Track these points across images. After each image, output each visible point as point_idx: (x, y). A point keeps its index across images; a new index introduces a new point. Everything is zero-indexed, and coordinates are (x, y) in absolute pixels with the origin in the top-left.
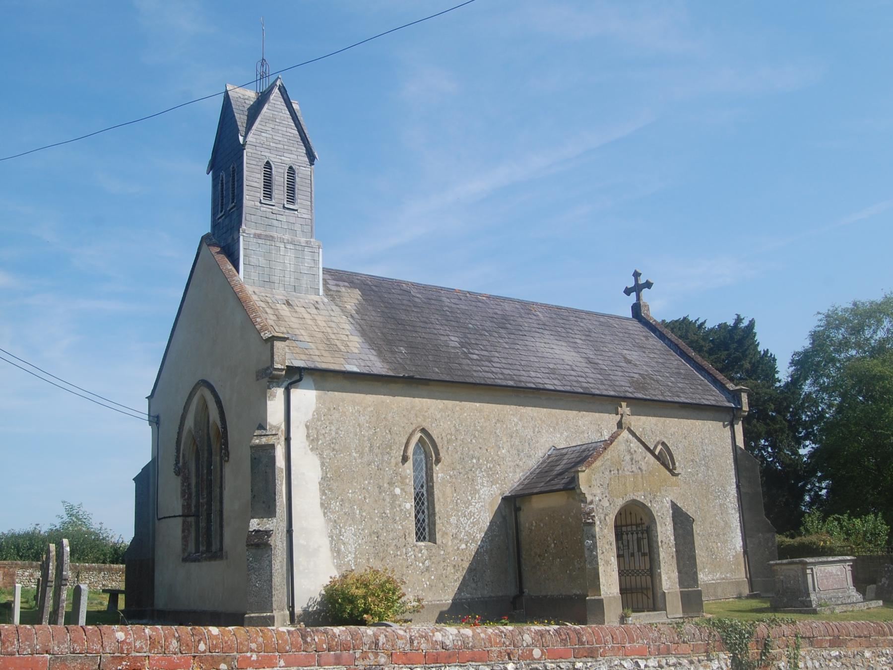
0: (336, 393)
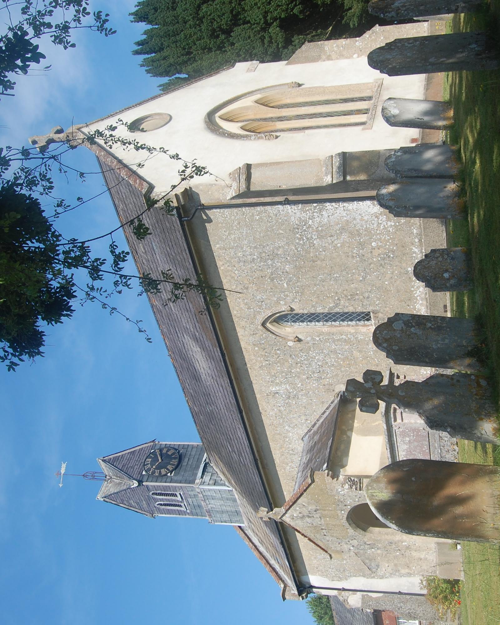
0: (307, 567)
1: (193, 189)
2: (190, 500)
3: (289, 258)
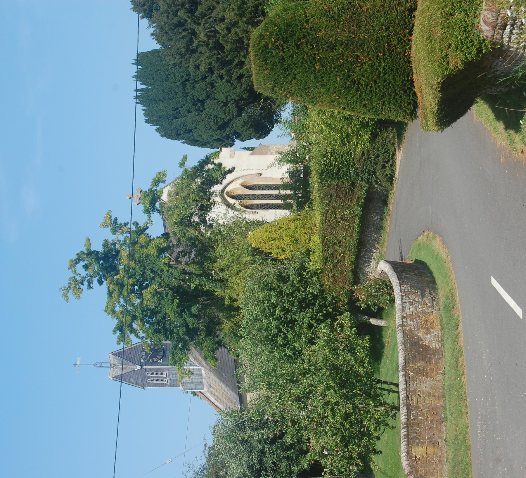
2: (171, 376)
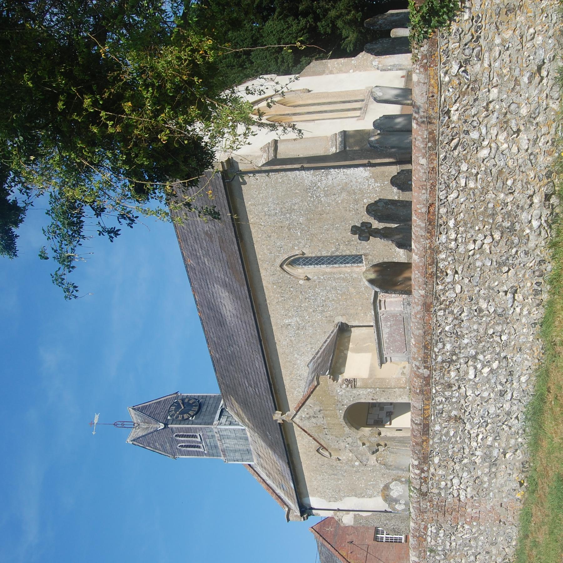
0: (308, 489)
1: (234, 159)
2: (208, 441)
3: (302, 212)
